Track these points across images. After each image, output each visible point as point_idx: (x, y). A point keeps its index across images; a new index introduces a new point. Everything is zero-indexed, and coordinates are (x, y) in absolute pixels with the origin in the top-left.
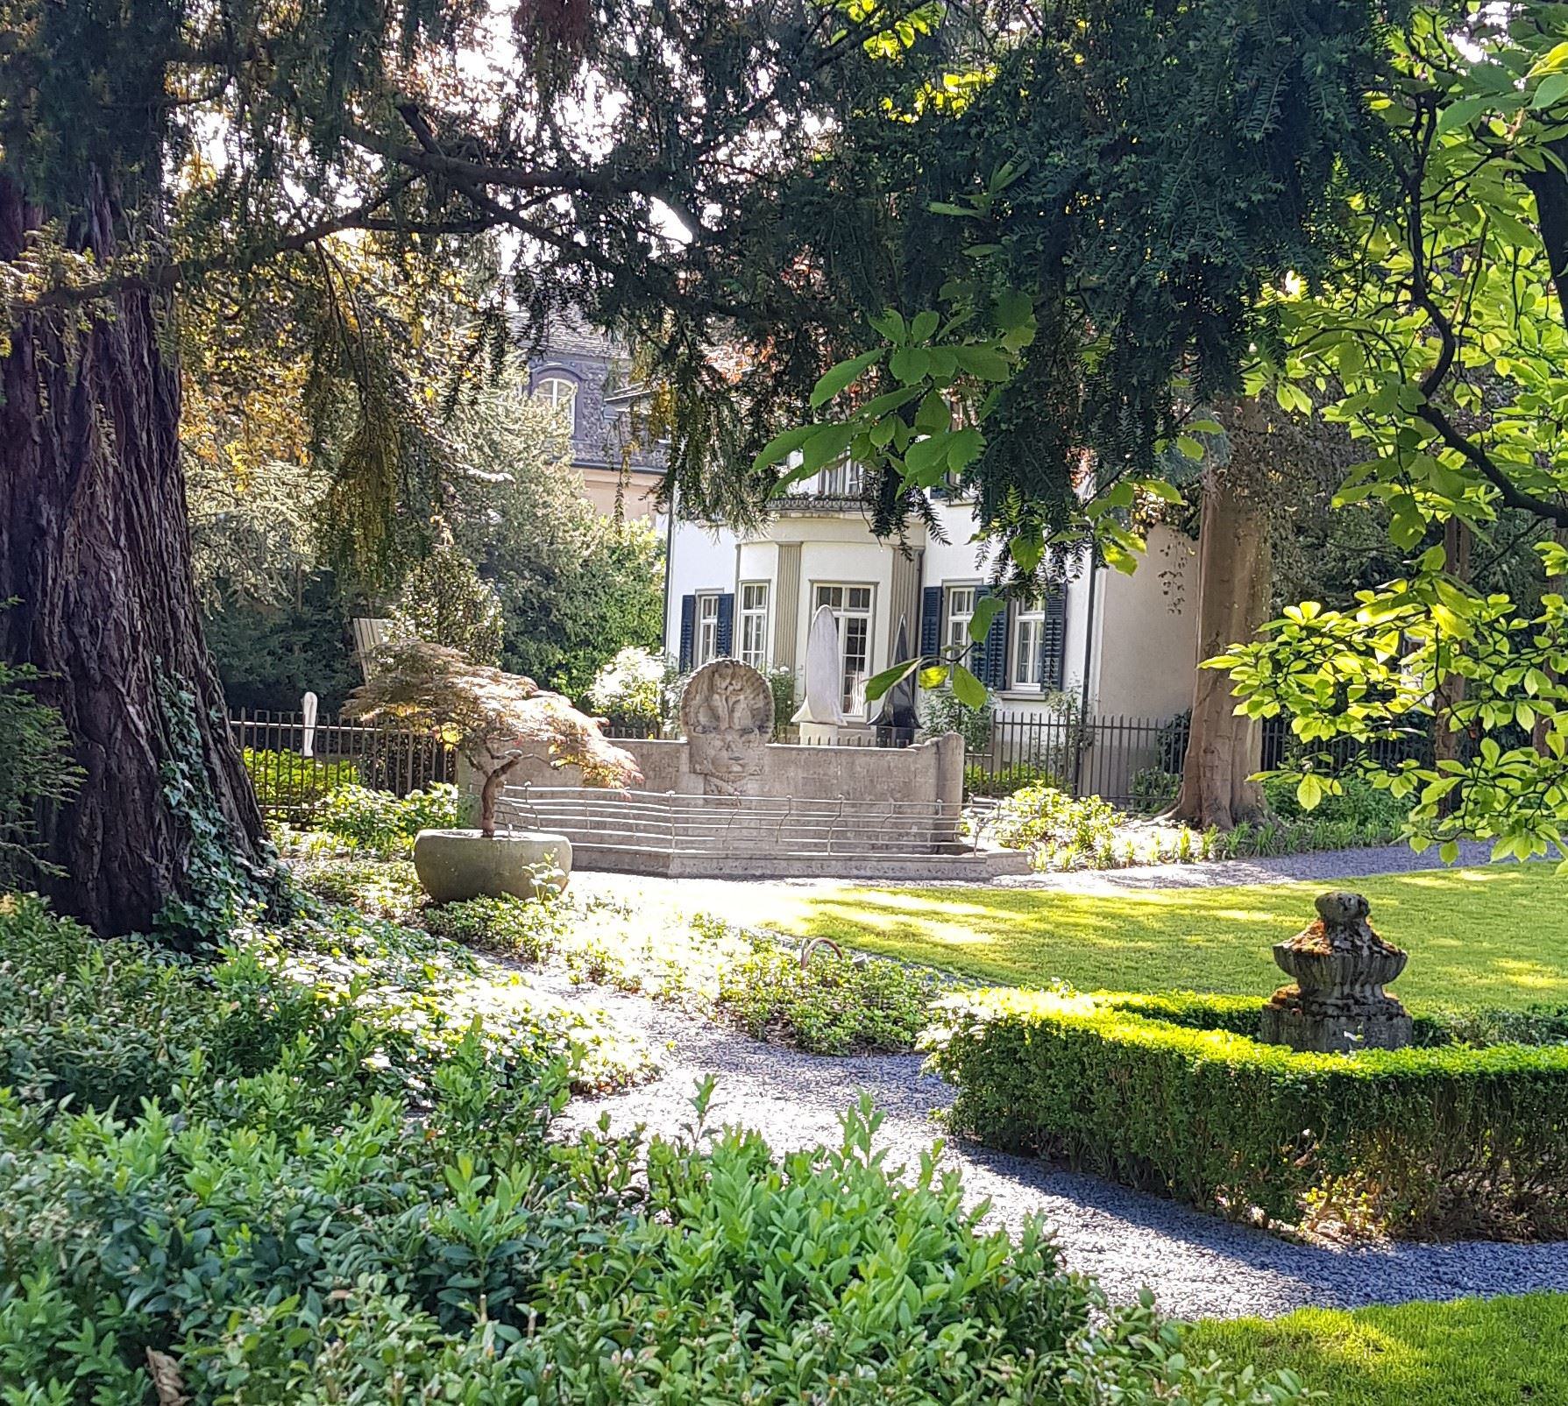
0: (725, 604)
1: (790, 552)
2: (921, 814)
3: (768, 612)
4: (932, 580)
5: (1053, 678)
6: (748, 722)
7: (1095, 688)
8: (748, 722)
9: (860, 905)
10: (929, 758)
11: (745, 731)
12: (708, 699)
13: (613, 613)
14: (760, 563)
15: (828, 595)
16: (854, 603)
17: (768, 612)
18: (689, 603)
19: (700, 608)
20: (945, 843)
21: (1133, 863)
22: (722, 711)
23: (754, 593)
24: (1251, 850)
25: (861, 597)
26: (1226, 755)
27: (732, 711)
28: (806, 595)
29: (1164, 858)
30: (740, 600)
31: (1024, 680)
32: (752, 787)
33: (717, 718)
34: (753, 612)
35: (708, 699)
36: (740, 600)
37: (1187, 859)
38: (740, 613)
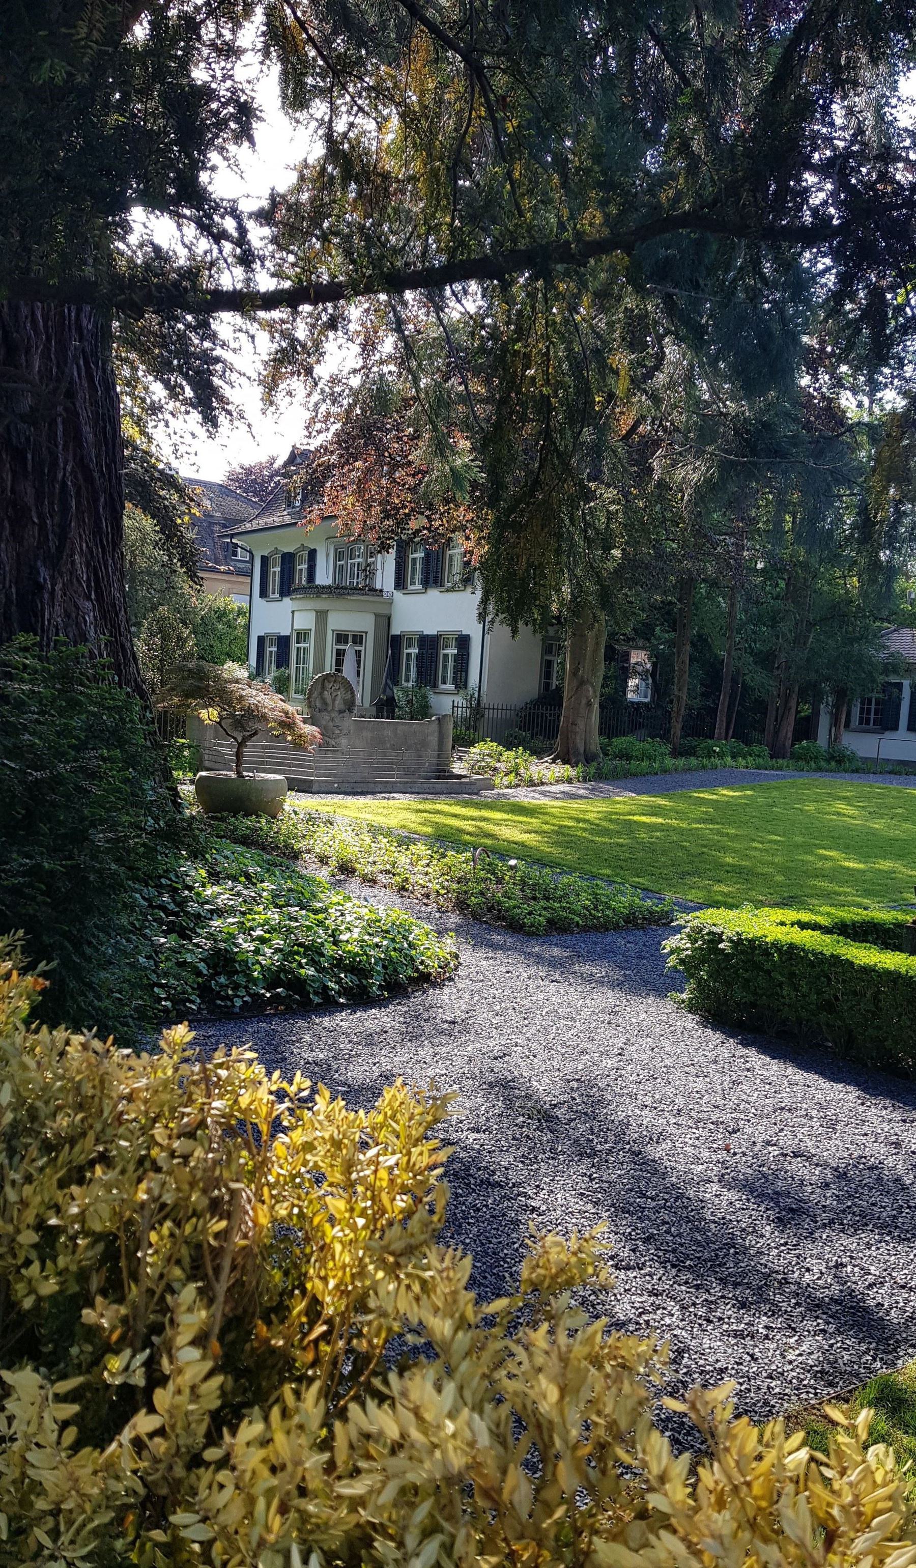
0: (283, 642)
1: (321, 616)
2: (430, 757)
3: (310, 645)
4: (396, 631)
5: (461, 682)
6: (342, 707)
7: (484, 687)
8: (342, 707)
9: (455, 816)
10: (435, 727)
11: (340, 712)
12: (321, 694)
13: (216, 644)
14: (305, 621)
15: (341, 638)
16: (354, 642)
17: (310, 645)
18: (261, 640)
19: (267, 643)
20: (442, 772)
21: (543, 784)
22: (329, 701)
23: (302, 636)
24: (600, 776)
25: (358, 639)
26: (582, 727)
27: (334, 701)
28: (330, 638)
29: (558, 781)
30: (294, 639)
31: (444, 683)
32: (344, 741)
33: (326, 704)
34: (302, 645)
35: (321, 694)
36: (294, 639)
37: (570, 781)
38: (294, 646)
